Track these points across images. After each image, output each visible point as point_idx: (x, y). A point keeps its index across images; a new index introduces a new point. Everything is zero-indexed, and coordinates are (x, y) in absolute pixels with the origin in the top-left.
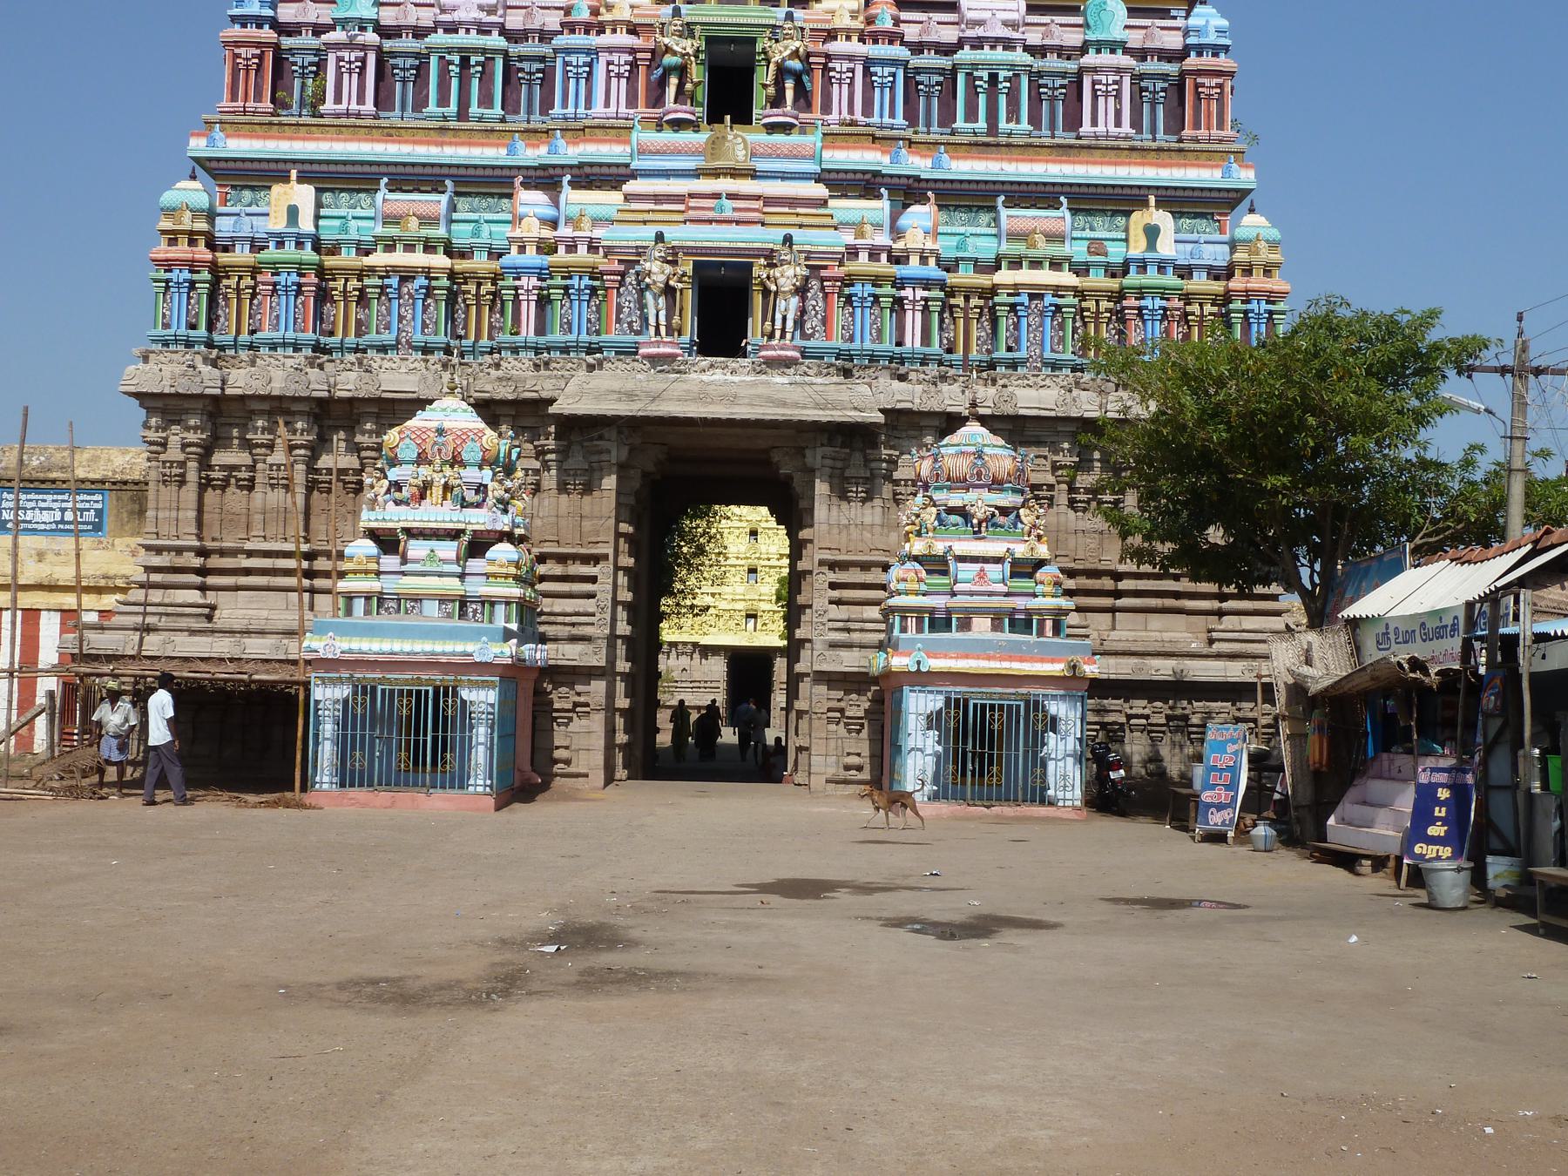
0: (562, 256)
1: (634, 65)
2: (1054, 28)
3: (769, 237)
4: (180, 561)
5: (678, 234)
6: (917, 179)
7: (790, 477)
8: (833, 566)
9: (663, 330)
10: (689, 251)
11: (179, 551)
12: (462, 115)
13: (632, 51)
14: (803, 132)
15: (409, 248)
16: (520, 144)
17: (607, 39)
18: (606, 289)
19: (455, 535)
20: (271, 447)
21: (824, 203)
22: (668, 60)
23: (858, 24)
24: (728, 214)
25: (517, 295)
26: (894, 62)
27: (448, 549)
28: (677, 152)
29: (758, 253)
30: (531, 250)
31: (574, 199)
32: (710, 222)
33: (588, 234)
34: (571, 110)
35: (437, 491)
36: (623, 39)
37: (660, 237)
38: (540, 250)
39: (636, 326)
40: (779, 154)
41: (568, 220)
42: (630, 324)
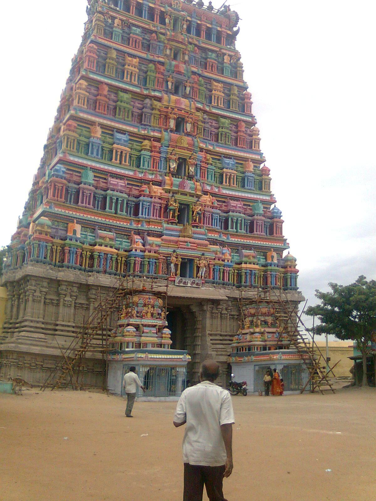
0: (147, 253)
1: (161, 207)
2: (248, 210)
3: (199, 254)
4: (38, 325)
5: (179, 251)
6: (223, 241)
7: (195, 312)
8: (211, 335)
9: (174, 274)
10: (181, 255)
11: (38, 322)
12: (116, 213)
13: (161, 204)
14: (200, 228)
15: (106, 246)
16: (133, 223)
17: (153, 200)
18: (159, 263)
19: (154, 326)
20: (65, 295)
21: (206, 246)
22: (171, 207)
23: (210, 204)
24: (189, 247)
25: (135, 262)
26: (217, 214)
27: (154, 330)
28: (176, 231)
29: (197, 257)
30: (138, 251)
31: (150, 239)
32: (185, 248)
33: (154, 248)
34: (144, 216)
35: (149, 314)
36: (157, 200)
37: (174, 251)
38: (141, 251)
39: (166, 273)
40: (200, 234)
41: (150, 245)
42: (165, 272)
